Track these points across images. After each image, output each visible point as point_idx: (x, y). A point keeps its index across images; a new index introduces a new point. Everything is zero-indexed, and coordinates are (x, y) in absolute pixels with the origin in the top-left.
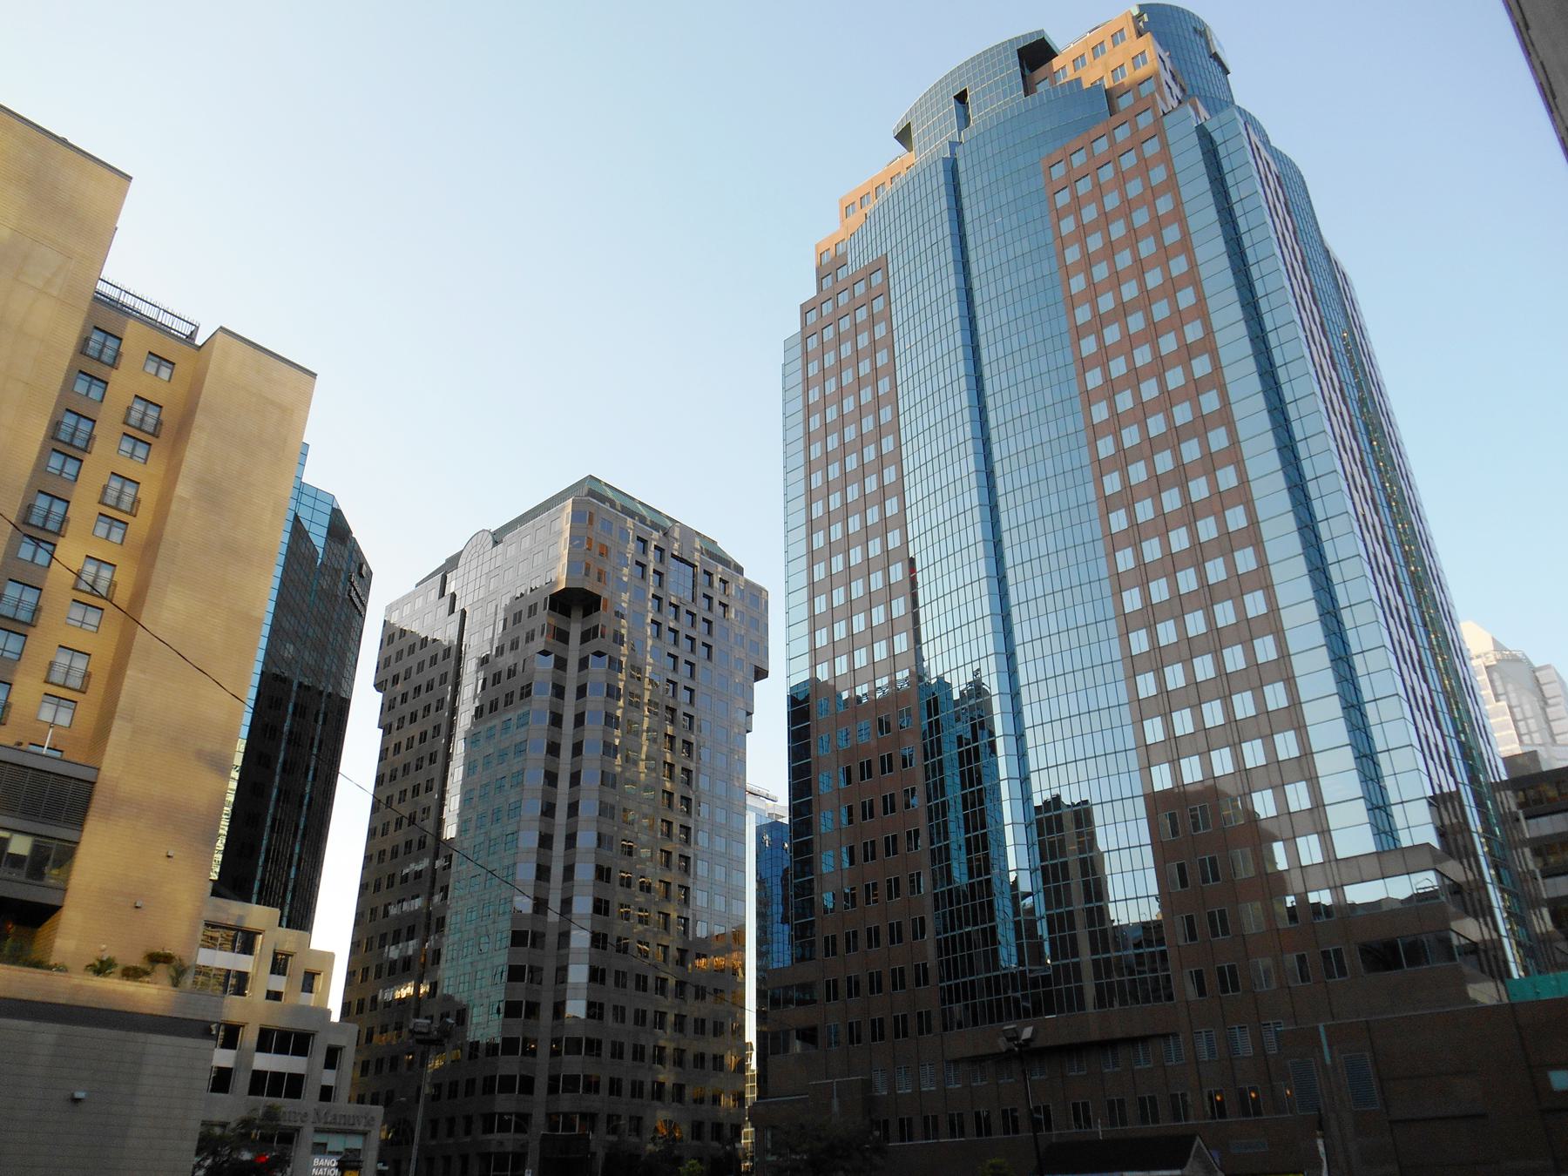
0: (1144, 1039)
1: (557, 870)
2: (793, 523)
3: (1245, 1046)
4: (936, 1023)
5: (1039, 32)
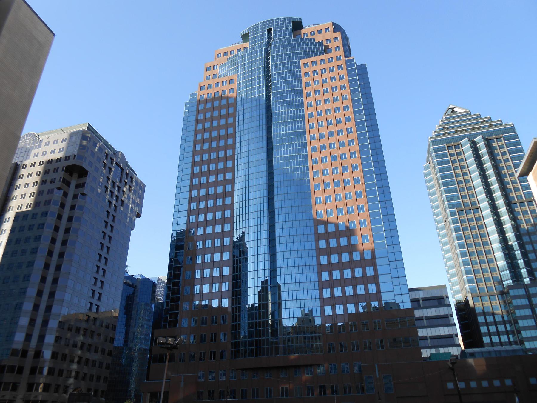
0: (311, 366)
1: (50, 279)
2: (186, 161)
5: (300, 19)
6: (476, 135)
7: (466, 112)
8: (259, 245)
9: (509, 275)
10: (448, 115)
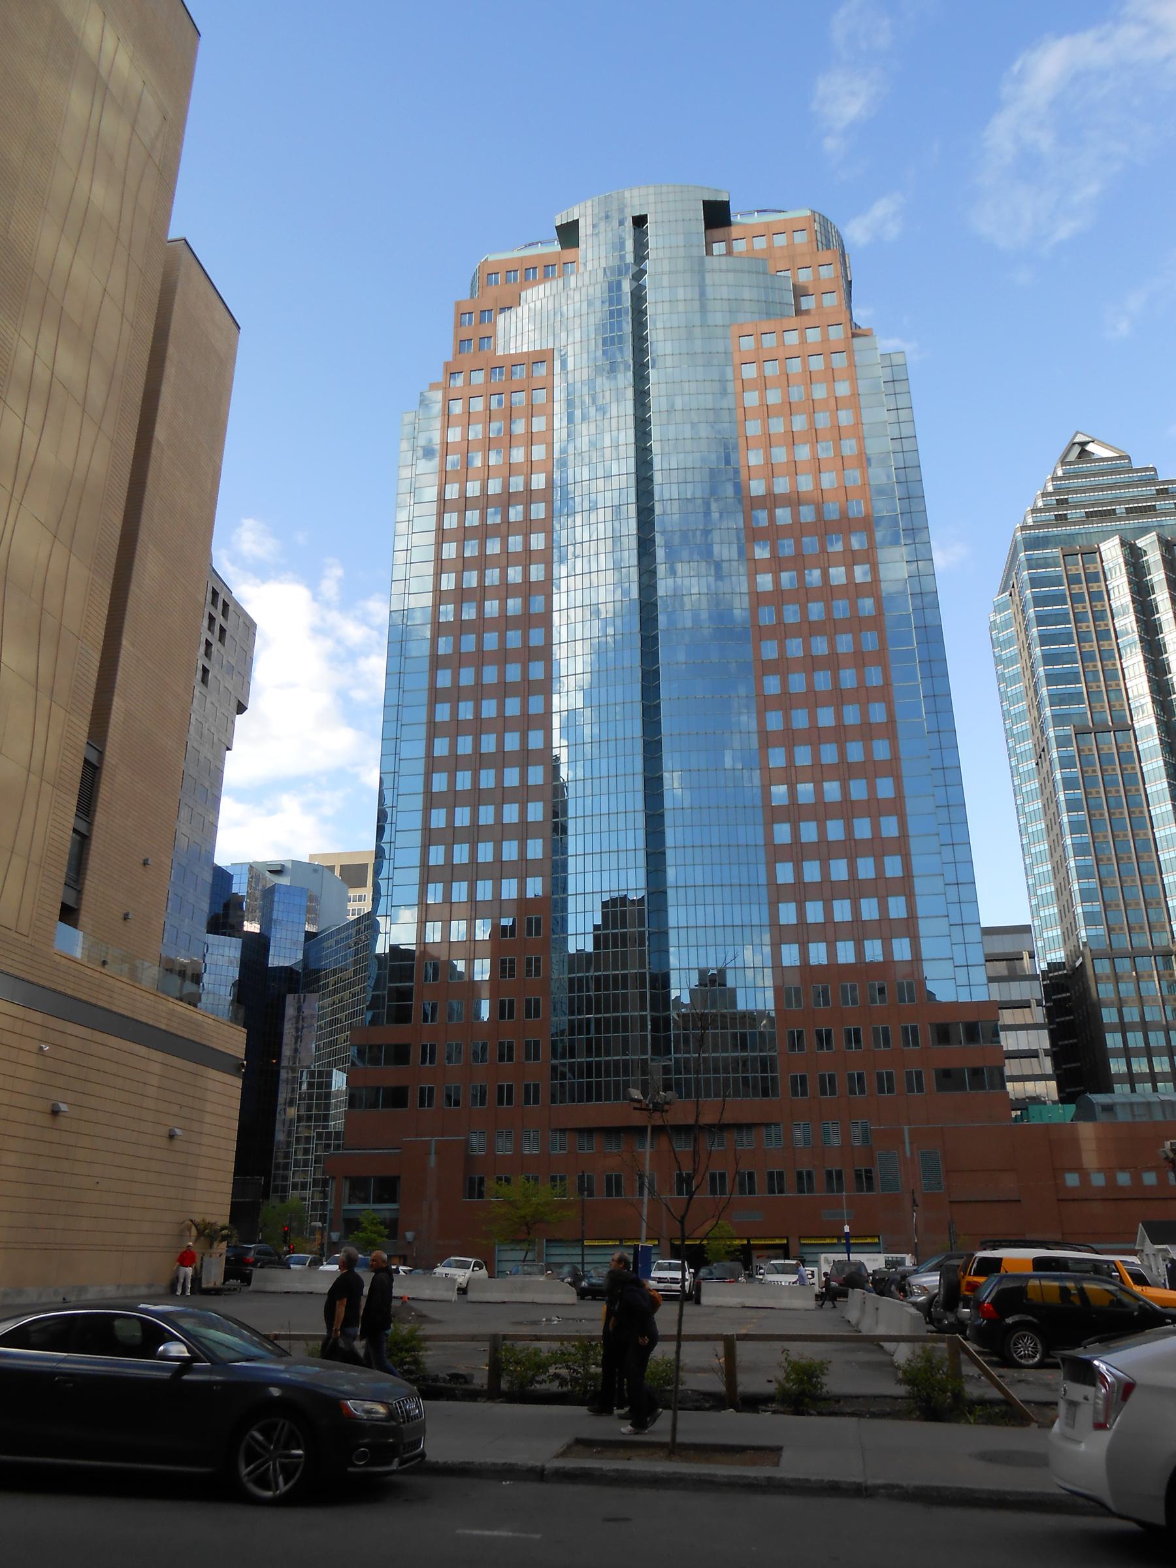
0: (750, 1126)
3: (835, 1139)
4: (544, 1095)
6: (1145, 531)
7: (1120, 458)
8: (622, 826)
10: (1070, 463)
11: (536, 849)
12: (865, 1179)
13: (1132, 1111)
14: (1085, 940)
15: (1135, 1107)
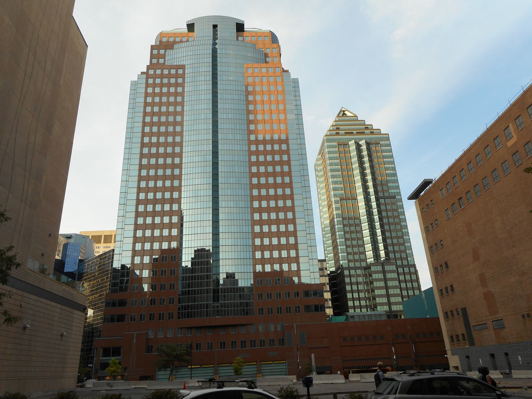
0: (245, 325)
3: (272, 328)
4: (175, 316)
9: (372, 254)
11: (175, 232)
12: (282, 341)
13: (359, 317)
14: (341, 264)
15: (360, 316)
